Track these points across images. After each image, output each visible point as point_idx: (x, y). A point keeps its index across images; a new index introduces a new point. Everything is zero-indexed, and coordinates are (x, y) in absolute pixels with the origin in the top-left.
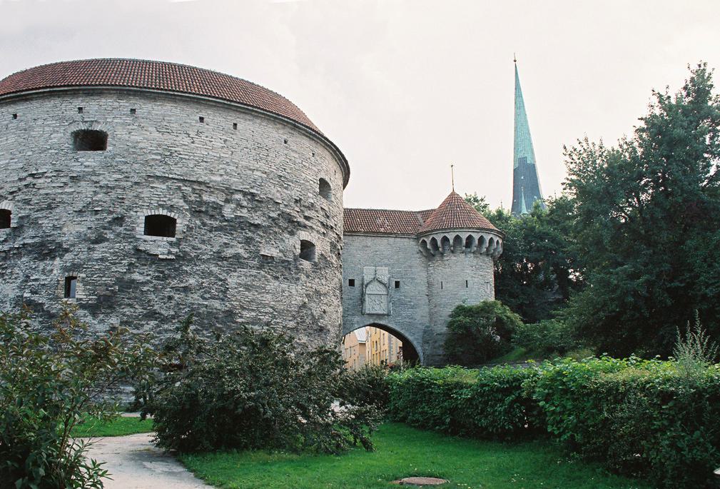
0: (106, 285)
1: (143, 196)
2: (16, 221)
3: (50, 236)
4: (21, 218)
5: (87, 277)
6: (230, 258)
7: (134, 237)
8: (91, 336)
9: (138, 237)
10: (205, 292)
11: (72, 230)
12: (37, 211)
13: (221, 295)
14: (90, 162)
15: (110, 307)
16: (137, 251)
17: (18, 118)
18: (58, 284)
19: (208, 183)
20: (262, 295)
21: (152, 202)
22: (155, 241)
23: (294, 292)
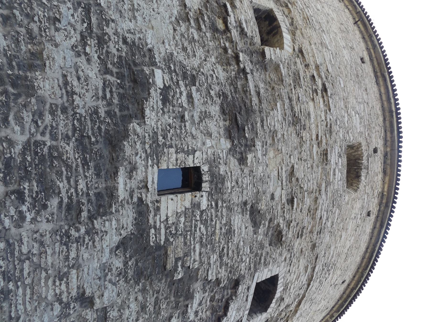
0: (186, 255)
1: (301, 261)
2: (273, 58)
3: (262, 126)
4: (277, 68)
5: (202, 212)
7: (255, 271)
8: (67, 258)
9: (257, 275)
11: (267, 163)
12: (290, 99)
14: (338, 175)
15: (139, 274)
16: (236, 284)
17: (362, 64)
18: (188, 153)
21: (292, 274)
22: (247, 300)
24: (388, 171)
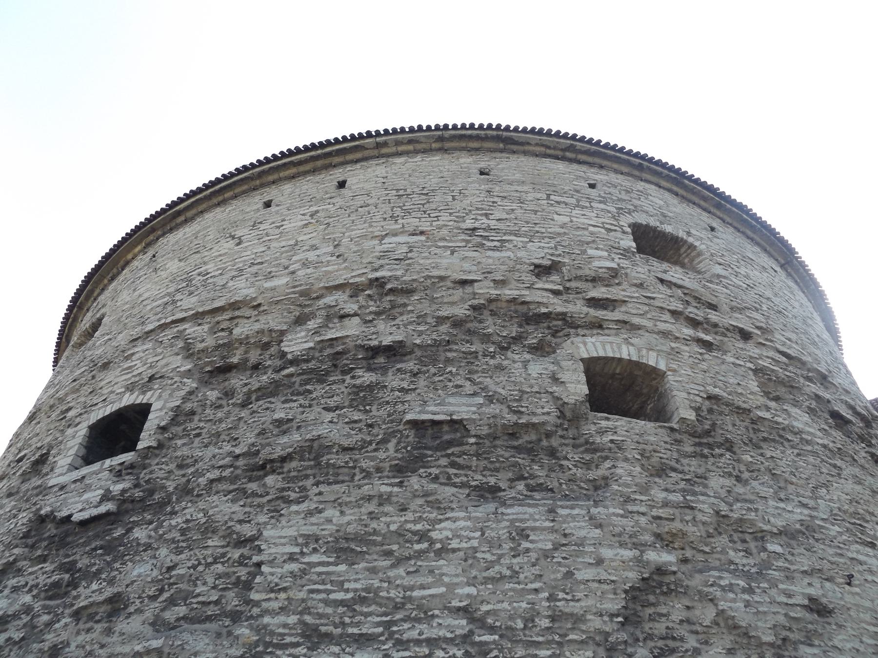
6: (284, 459)
10: (172, 602)
13: (232, 600)
19: (255, 299)
20: (411, 566)
23: (581, 530)
24: (122, 263)
